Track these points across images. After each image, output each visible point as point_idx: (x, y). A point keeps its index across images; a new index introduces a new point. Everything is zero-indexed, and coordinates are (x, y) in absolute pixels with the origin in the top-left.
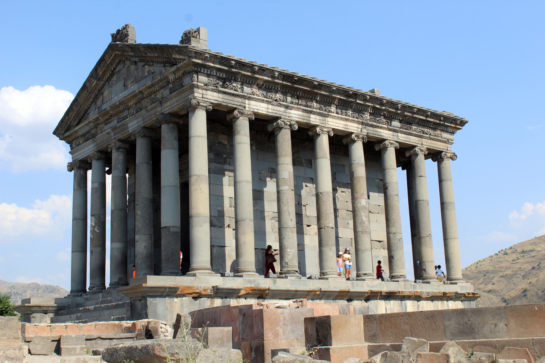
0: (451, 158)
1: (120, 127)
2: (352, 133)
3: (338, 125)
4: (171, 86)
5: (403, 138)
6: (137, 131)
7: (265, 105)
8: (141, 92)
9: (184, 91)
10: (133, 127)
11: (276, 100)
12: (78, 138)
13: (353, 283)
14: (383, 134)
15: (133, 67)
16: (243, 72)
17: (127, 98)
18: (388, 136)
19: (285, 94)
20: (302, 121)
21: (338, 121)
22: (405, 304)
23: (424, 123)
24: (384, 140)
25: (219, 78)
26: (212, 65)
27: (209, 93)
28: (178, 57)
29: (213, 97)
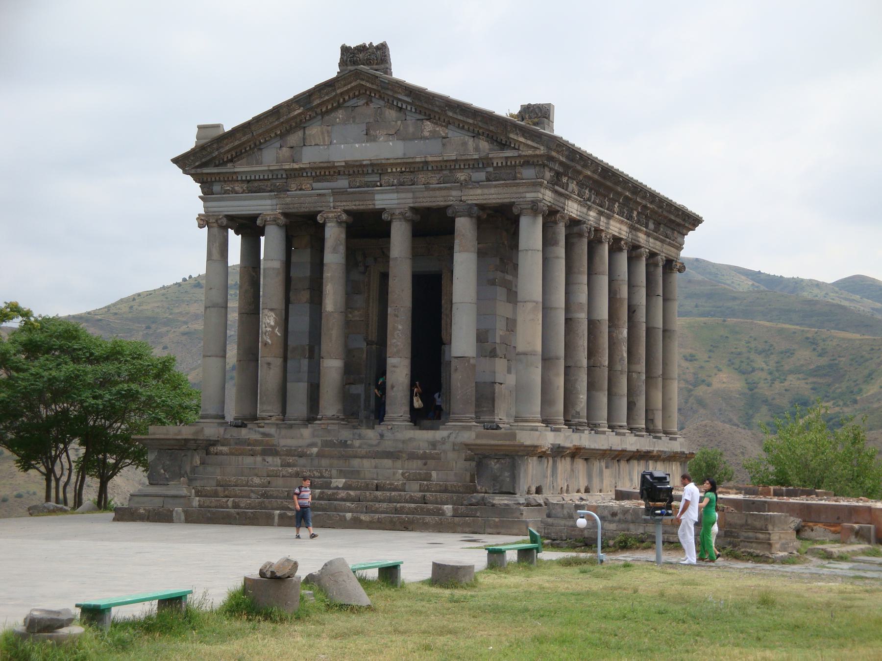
0: (680, 271)
1: (352, 193)
2: (621, 239)
4: (490, 169)
6: (397, 212)
7: (575, 206)
8: (426, 163)
9: (517, 185)
10: (388, 202)
12: (232, 180)
14: (641, 240)
15: (391, 114)
17: (391, 161)
24: (639, 247)
28: (522, 139)
29: (547, 196)
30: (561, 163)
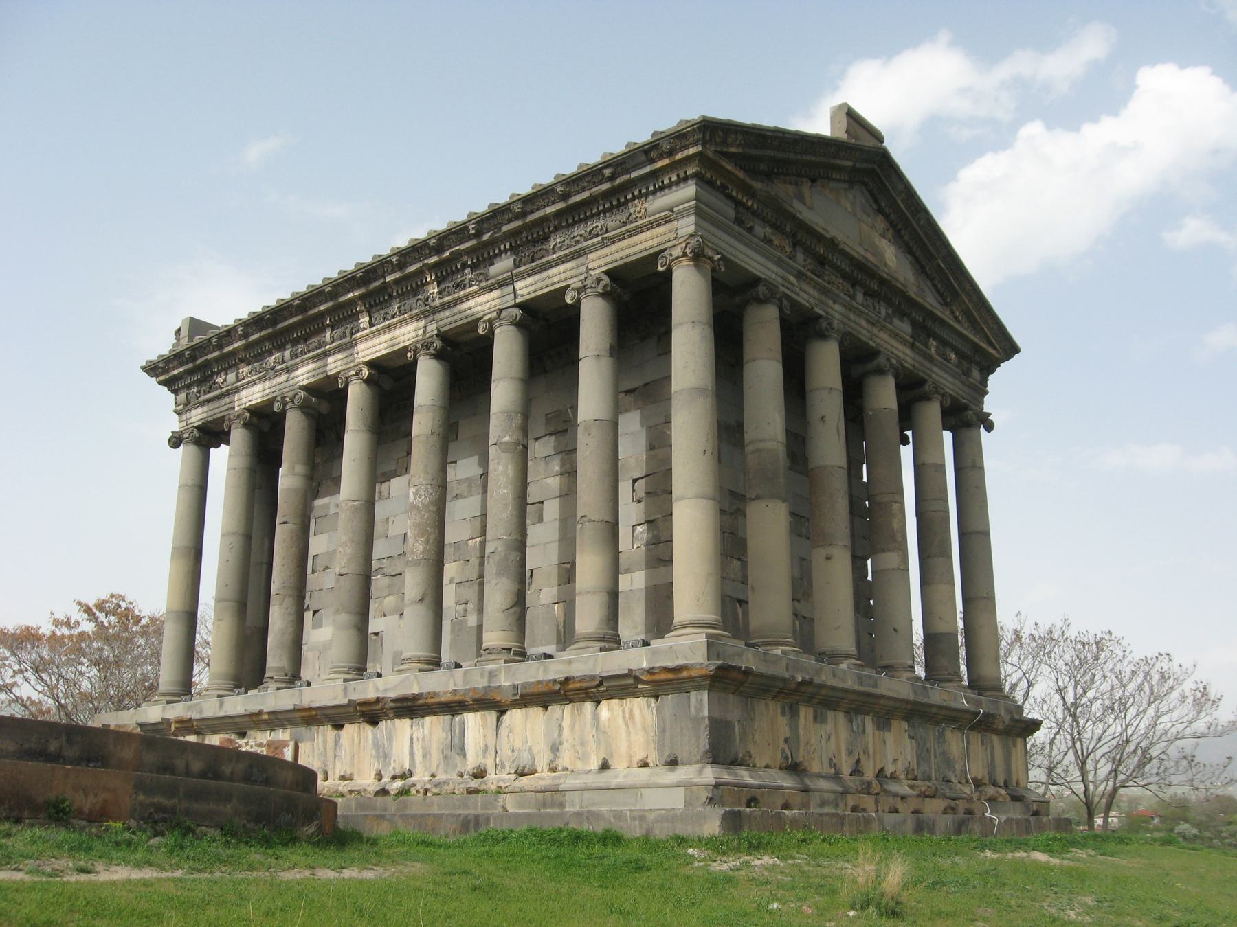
3: (377, 348)
5: (527, 288)
7: (258, 387)
11: (273, 369)
13: (346, 688)
16: (210, 357)
18: (488, 305)
19: (281, 348)
20: (313, 380)
21: (376, 341)
22: (462, 724)
23: (574, 215)
25: (200, 383)
26: (175, 372)
27: (194, 412)
29: (198, 415)
30: (190, 372)
